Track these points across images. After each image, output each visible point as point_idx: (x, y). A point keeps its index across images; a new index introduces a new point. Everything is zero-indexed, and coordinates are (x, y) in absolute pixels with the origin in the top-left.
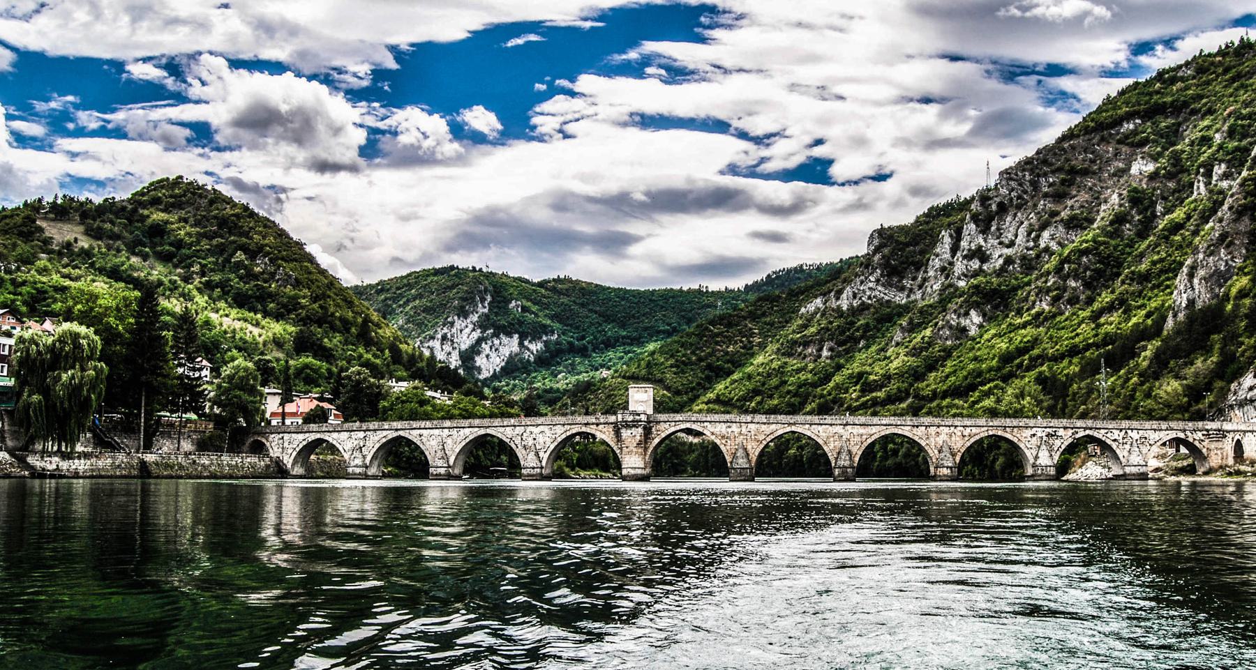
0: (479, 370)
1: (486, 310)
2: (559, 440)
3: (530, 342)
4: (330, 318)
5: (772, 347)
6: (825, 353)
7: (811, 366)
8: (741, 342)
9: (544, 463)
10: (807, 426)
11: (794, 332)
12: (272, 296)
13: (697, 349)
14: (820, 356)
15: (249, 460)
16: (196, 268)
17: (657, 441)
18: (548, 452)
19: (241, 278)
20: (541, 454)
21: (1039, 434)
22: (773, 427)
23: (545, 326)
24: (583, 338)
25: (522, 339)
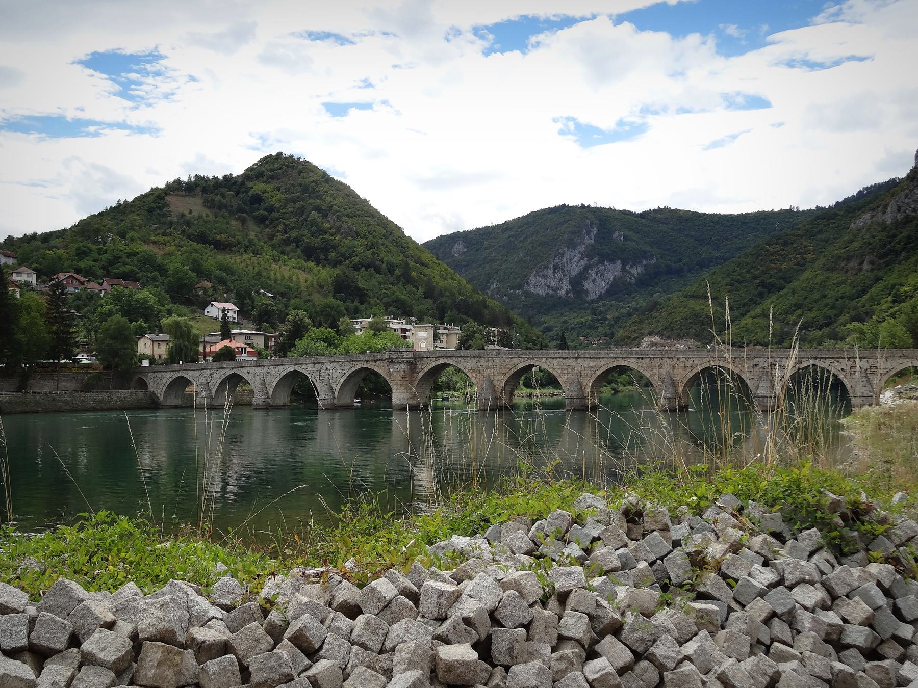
0: (587, 292)
1: (592, 241)
2: (347, 374)
3: (631, 266)
4: (377, 263)
5: (819, 263)
6: (866, 266)
7: (850, 280)
8: (795, 259)
9: (336, 395)
10: (544, 360)
11: (840, 247)
12: (334, 247)
13: (753, 267)
14: (861, 270)
15: (118, 395)
16: (280, 227)
17: (421, 374)
18: (340, 385)
19: (313, 234)
20: (334, 387)
21: (761, 365)
22: (515, 360)
23: (645, 252)
24: (680, 260)
25: (624, 263)
